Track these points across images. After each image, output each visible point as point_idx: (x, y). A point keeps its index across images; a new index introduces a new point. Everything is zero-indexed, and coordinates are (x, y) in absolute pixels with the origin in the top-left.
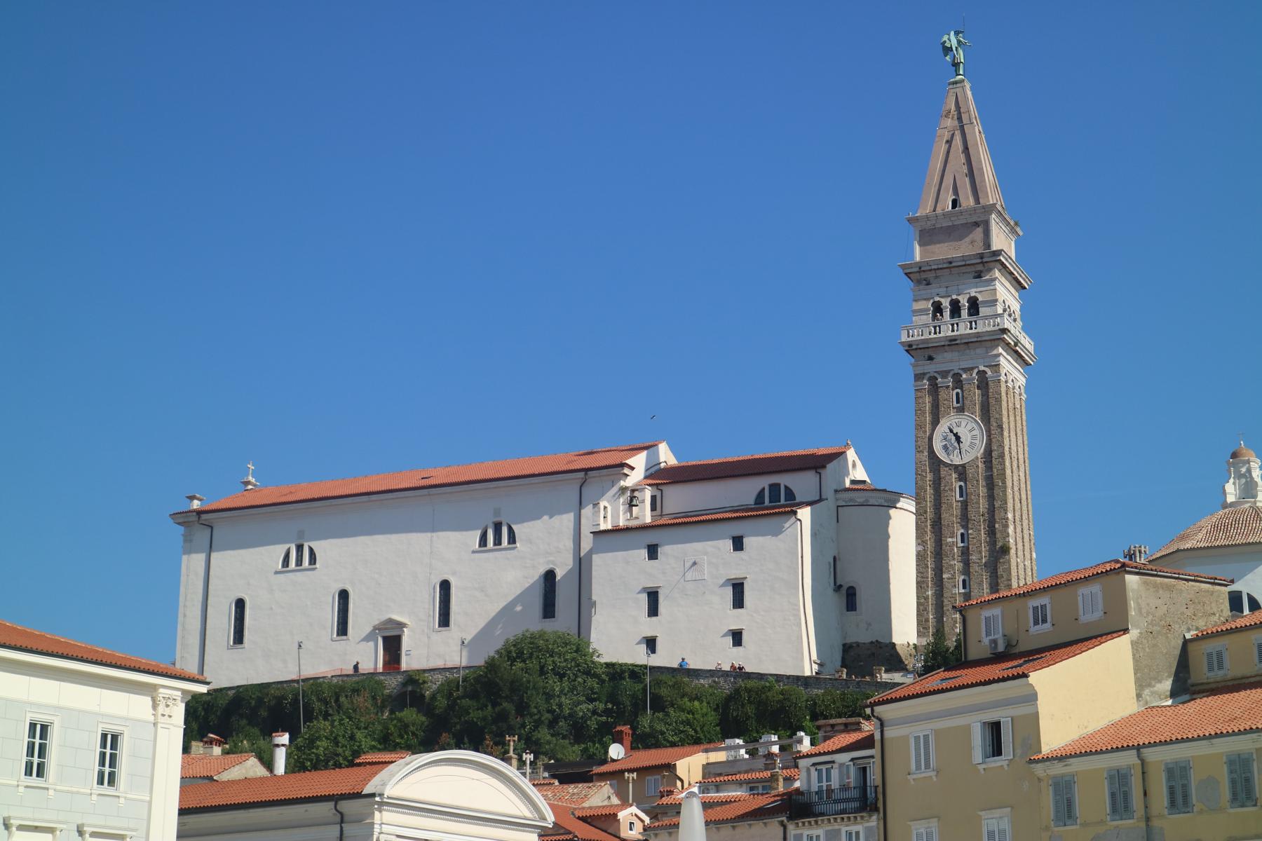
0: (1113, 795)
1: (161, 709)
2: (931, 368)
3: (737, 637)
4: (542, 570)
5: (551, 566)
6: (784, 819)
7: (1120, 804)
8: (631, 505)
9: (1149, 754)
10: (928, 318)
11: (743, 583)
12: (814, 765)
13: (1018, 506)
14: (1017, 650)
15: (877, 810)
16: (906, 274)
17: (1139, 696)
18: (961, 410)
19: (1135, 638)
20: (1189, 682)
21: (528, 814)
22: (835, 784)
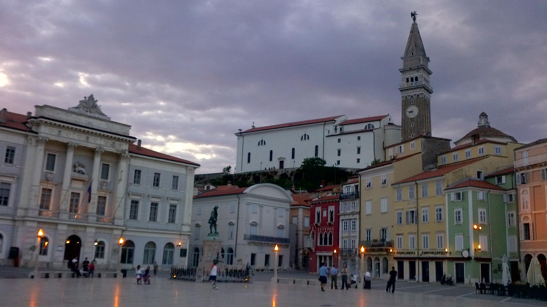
0: (410, 193)
1: (188, 172)
2: (406, 95)
3: (358, 161)
4: (315, 146)
5: (316, 145)
6: (339, 200)
7: (411, 196)
8: (336, 129)
9: (418, 182)
10: (405, 82)
11: (360, 148)
12: (346, 187)
13: (427, 128)
14: (396, 158)
15: (358, 197)
16: (401, 72)
17: (423, 169)
18: (413, 105)
19: (423, 154)
20: (438, 165)
21: (287, 199)
22: (351, 191)
